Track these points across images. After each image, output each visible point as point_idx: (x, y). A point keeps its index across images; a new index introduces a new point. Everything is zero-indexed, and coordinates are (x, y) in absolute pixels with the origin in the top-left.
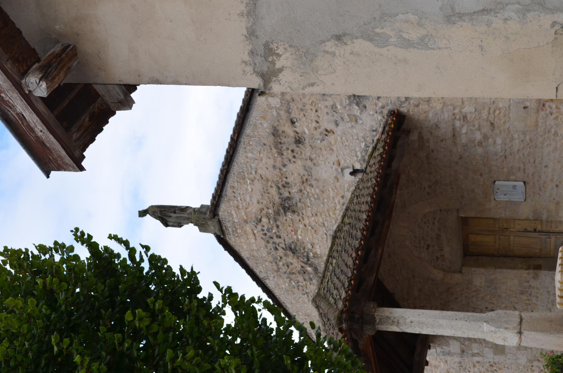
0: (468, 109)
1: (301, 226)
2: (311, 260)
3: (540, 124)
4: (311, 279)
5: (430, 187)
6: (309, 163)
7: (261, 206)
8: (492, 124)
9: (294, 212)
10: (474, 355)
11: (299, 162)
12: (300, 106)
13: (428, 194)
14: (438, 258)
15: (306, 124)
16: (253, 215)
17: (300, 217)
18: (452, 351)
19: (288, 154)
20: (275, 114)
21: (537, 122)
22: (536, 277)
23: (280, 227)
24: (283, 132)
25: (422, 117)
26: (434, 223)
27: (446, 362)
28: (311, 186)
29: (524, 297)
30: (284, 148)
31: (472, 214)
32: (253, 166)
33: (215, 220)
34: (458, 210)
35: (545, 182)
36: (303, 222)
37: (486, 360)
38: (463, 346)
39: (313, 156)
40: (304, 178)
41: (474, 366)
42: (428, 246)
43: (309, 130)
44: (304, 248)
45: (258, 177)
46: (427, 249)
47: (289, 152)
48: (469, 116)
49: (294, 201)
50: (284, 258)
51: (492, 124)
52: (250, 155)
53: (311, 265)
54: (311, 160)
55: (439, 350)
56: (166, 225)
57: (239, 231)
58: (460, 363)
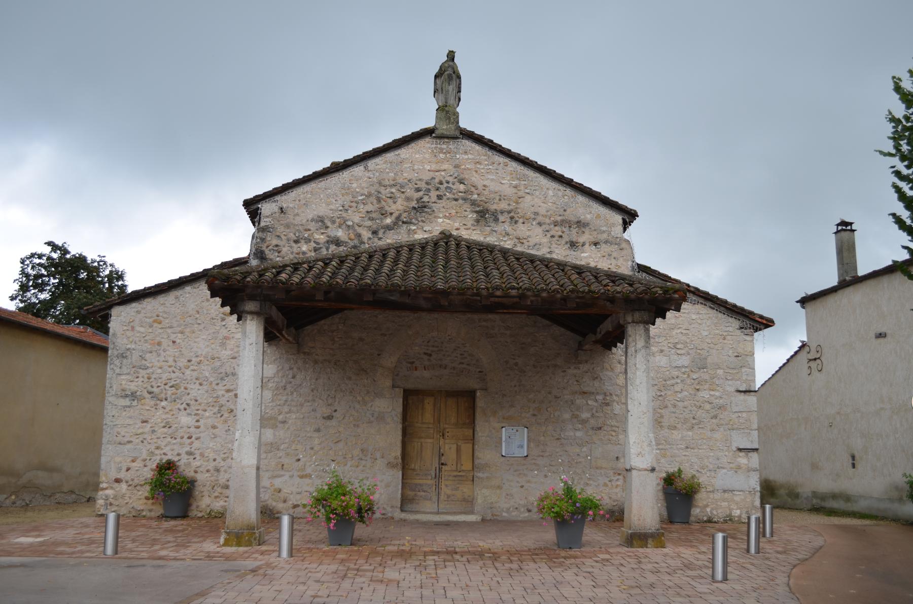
0: (617, 408)
1: (457, 225)
2: (405, 226)
3: (598, 471)
5: (516, 364)
7: (480, 187)
8: (600, 428)
9: (478, 221)
11: (545, 240)
12: (614, 254)
13: (507, 362)
14: (413, 363)
15: (593, 256)
16: (467, 177)
17: (469, 226)
19: (557, 231)
20: (604, 229)
21: (601, 468)
22: (391, 465)
23: (455, 202)
24: (584, 232)
25: (607, 365)
29: (356, 452)
30: (564, 229)
31: (480, 403)
32: (537, 193)
33: (457, 133)
35: (525, 475)
36: (462, 228)
40: (524, 241)
41: (228, 391)
42: (430, 355)
43: (585, 258)
44: (423, 221)
45: (520, 194)
46: (425, 354)
47: (560, 233)
48: (609, 408)
50: (403, 196)
51: (600, 428)
53: (395, 223)
56: (436, 77)
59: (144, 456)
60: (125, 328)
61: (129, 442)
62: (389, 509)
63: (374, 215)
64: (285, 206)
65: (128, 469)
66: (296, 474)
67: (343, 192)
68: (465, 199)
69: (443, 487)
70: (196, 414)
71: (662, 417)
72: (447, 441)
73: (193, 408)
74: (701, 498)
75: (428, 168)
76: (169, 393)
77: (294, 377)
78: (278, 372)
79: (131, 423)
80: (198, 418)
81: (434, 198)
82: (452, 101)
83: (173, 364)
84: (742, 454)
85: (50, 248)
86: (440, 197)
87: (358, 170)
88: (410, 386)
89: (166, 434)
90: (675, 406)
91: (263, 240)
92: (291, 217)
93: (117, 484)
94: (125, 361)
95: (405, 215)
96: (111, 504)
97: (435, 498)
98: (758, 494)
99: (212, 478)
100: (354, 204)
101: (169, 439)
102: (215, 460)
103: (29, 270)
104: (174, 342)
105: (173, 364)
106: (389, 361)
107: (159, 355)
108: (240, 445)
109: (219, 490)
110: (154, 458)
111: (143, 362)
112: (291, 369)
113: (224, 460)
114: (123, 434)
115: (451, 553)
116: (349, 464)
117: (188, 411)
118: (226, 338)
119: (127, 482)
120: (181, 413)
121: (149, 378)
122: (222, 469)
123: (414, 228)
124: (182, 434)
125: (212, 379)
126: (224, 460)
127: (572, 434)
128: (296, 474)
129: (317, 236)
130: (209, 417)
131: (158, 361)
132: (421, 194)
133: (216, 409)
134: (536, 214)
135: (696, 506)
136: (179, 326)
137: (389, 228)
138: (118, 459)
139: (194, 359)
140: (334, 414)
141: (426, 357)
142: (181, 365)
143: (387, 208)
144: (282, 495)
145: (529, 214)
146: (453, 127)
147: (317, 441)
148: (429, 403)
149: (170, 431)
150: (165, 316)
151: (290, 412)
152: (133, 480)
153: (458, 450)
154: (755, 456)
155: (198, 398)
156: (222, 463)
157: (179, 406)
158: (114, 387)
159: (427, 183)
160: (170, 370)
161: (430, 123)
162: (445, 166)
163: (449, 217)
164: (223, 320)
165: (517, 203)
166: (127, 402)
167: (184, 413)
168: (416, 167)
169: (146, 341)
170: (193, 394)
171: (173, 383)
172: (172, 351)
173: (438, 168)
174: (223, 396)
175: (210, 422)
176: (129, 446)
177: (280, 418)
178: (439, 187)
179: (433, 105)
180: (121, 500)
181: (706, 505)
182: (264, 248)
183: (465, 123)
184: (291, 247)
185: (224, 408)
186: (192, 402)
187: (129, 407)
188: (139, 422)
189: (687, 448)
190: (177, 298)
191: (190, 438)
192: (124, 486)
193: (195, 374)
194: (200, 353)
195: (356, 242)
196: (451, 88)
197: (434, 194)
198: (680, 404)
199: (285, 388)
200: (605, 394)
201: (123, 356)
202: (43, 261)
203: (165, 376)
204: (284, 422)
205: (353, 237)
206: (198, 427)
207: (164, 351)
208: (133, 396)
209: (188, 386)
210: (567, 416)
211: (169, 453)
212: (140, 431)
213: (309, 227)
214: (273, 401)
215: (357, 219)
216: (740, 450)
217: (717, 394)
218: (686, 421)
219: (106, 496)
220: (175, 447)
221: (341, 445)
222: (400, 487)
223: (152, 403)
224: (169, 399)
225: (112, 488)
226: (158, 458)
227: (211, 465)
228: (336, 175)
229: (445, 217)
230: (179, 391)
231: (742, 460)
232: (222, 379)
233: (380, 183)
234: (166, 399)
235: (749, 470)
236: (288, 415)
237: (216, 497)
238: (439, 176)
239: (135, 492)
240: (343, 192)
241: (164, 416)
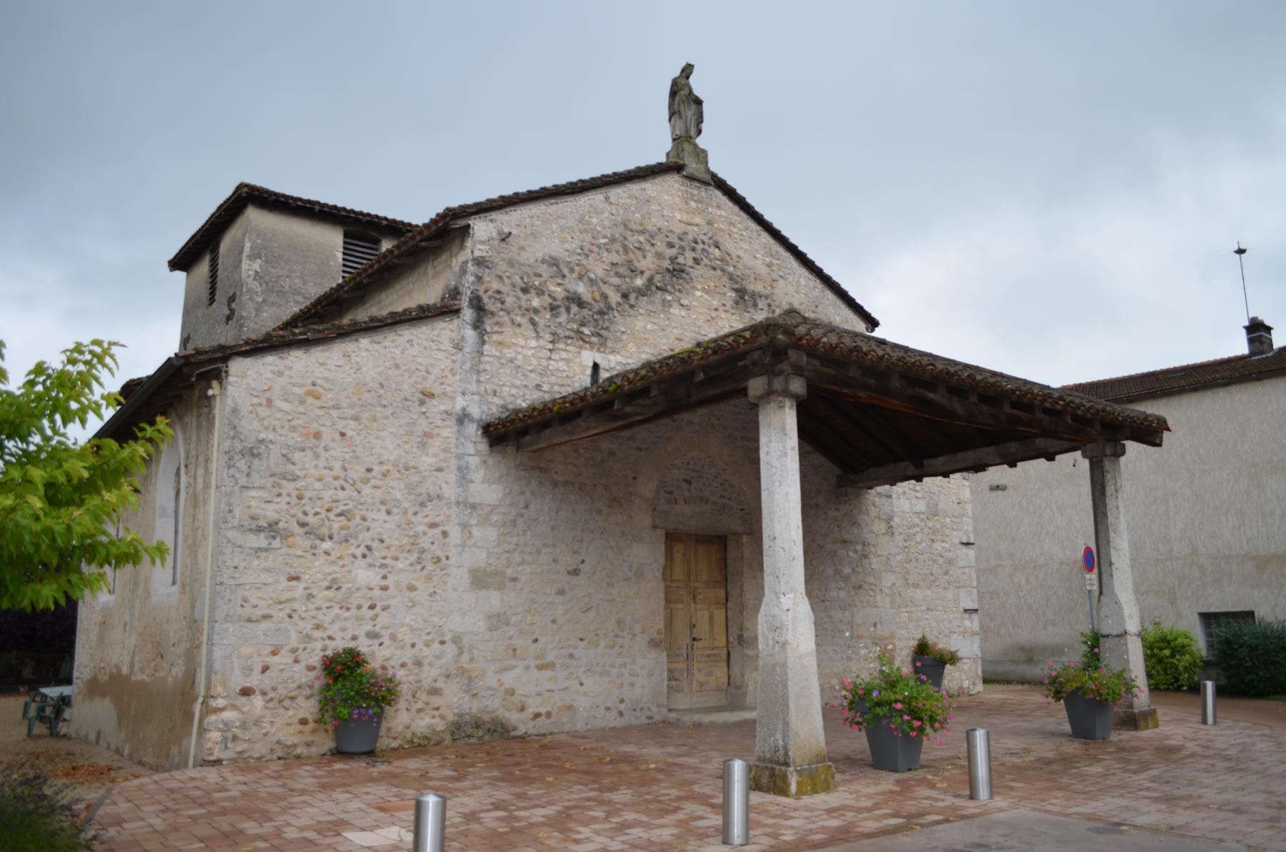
2: (660, 293)
7: (735, 259)
8: (860, 587)
9: (737, 303)
10: (464, 526)
14: (671, 493)
17: (728, 308)
18: (472, 486)
22: (654, 644)
26: (722, 497)
27: (440, 470)
33: (708, 178)
37: (453, 553)
38: (487, 510)
41: (433, 525)
44: (680, 291)
45: (774, 275)
46: (685, 480)
49: (751, 310)
58: (439, 497)
59: (294, 641)
60: (255, 400)
61: (266, 617)
62: (655, 709)
63: (621, 270)
65: (265, 669)
66: (533, 663)
67: (581, 227)
68: (723, 270)
69: (695, 672)
70: (382, 566)
72: (699, 606)
73: (377, 554)
75: (679, 217)
76: (336, 526)
77: (526, 507)
78: (505, 495)
79: (270, 580)
80: (384, 571)
81: (691, 262)
82: (693, 132)
83: (342, 474)
87: (596, 198)
89: (331, 600)
92: (515, 250)
93: (244, 699)
94: (256, 462)
95: (658, 277)
96: (235, 738)
99: (411, 678)
100: (594, 248)
101: (336, 611)
102: (413, 646)
104: (343, 434)
105: (342, 474)
106: (647, 488)
107: (317, 456)
108: (794, 619)
109: (423, 697)
110: (309, 646)
111: (290, 467)
112: (523, 493)
113: (427, 645)
114: (253, 601)
116: (602, 644)
117: (369, 560)
118: (427, 435)
119: (264, 693)
120: (357, 562)
121: (300, 498)
122: (426, 661)
123: (669, 298)
124: (359, 601)
125: (406, 505)
127: (835, 594)
128: (533, 663)
129: (553, 288)
130: (401, 571)
131: (316, 467)
136: (351, 406)
138: (245, 651)
139: (376, 468)
140: (582, 567)
141: (685, 486)
142: (355, 476)
143: (636, 263)
144: (515, 699)
147: (561, 610)
149: (339, 595)
150: (327, 385)
152: (274, 689)
153: (711, 618)
154: (975, 617)
155: (385, 537)
156: (426, 651)
157: (352, 550)
158: (237, 512)
159: (680, 239)
160: (337, 484)
162: (697, 220)
164: (422, 403)
165: (772, 287)
166: (261, 541)
167: (361, 562)
168: (665, 213)
169: (294, 429)
170: (377, 528)
171: (341, 508)
172: (339, 450)
173: (689, 220)
174: (425, 533)
175: (405, 579)
176: (265, 625)
177: (509, 572)
180: (254, 729)
182: (481, 293)
184: (518, 298)
185: (427, 556)
186: (375, 544)
187: (266, 550)
188: (283, 578)
190: (346, 355)
191: (372, 607)
192: (258, 701)
193: (379, 494)
194: (385, 458)
195: (602, 305)
197: (689, 255)
198: (921, 557)
199: (514, 523)
203: (328, 495)
205: (598, 297)
206: (385, 588)
207: (326, 449)
208: (272, 529)
209: (368, 514)
210: (830, 571)
211: (338, 636)
212: (287, 595)
213: (539, 271)
214: (498, 545)
216: (966, 611)
217: (947, 546)
219: (226, 724)
220: (349, 624)
221: (592, 615)
223: (308, 543)
224: (336, 538)
225: (234, 707)
226: (319, 645)
228: (570, 199)
229: (703, 290)
230: (352, 524)
232: (422, 505)
233: (626, 226)
234: (331, 538)
236: (519, 569)
237: (419, 711)
238: (693, 232)
239: (281, 711)
240: (581, 227)
241: (328, 569)
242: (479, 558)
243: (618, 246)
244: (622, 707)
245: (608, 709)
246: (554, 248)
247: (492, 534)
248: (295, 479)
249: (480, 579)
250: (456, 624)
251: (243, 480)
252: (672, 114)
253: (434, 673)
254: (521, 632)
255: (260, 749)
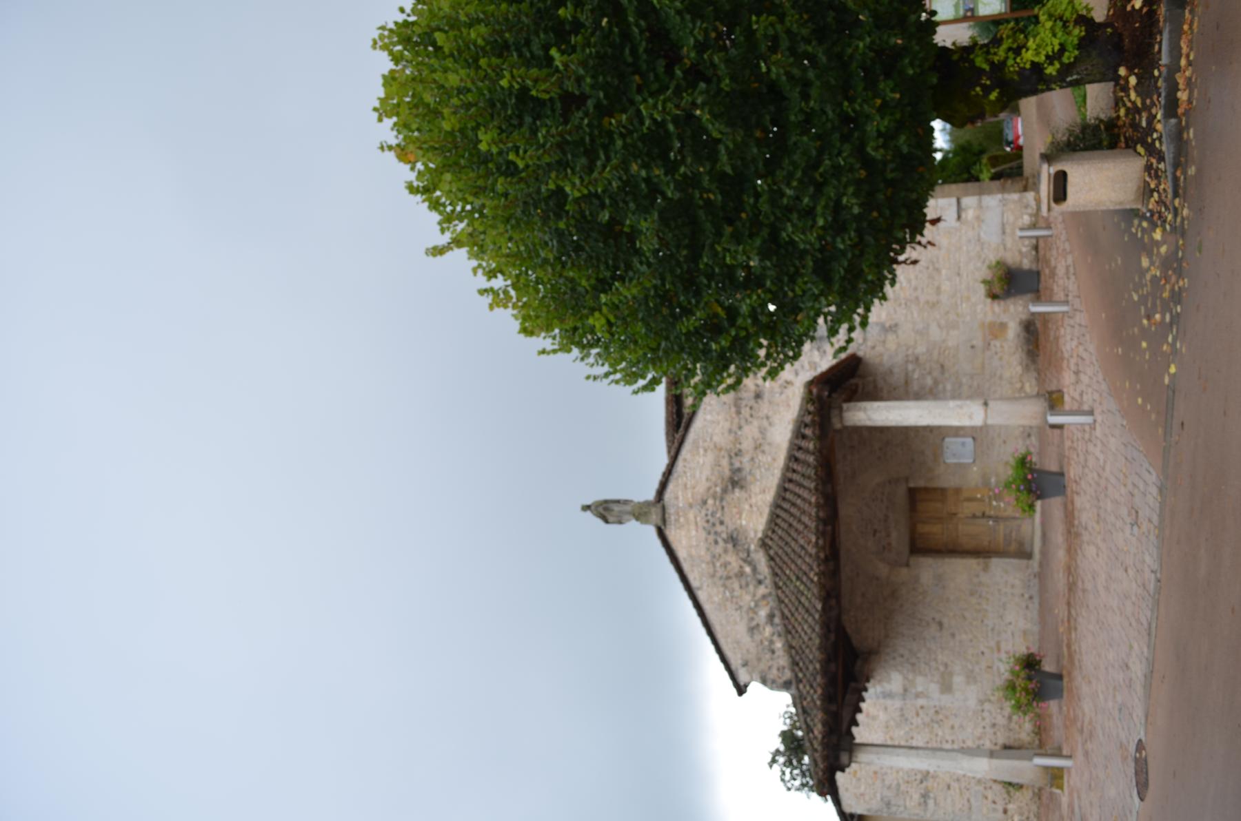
1: (747, 507)
2: (752, 555)
4: (747, 585)
5: (880, 449)
6: (765, 423)
7: (708, 484)
8: (942, 366)
9: (742, 487)
10: (917, 696)
14: (884, 548)
16: (699, 497)
19: (746, 412)
22: (986, 569)
25: (877, 361)
27: (886, 709)
28: (763, 452)
29: (974, 600)
33: (659, 505)
34: (907, 480)
39: (770, 414)
41: (918, 714)
45: (712, 446)
49: (744, 473)
52: (709, 417)
53: (750, 563)
54: (768, 418)
55: (879, 689)
56: (607, 522)
57: (682, 520)
58: (902, 709)
59: (981, 788)
63: (743, 583)
64: (740, 662)
65: (994, 802)
68: (722, 499)
71: (927, 302)
74: (1012, 258)
77: (902, 656)
82: (628, 508)
84: (963, 215)
85: (775, 766)
86: (722, 523)
87: (702, 596)
88: (906, 550)
90: (916, 289)
91: (773, 682)
93: (1009, 813)
94: (893, 802)
97: (1019, 522)
98: (1006, 196)
103: (797, 783)
106: (883, 570)
115: (1072, 587)
126: (983, 719)
132: (720, 540)
133: (936, 726)
134: (730, 431)
135: (1021, 262)
137: (754, 570)
138: (985, 811)
141: (878, 535)
145: (731, 438)
146: (653, 510)
147: (964, 636)
148: (923, 529)
151: (935, 660)
156: (987, 721)
161: (651, 531)
162: (691, 516)
163: (740, 513)
165: (721, 449)
166: (931, 802)
176: (972, 800)
177: (942, 668)
178: (712, 525)
179: (633, 525)
181: (1018, 255)
183: (651, 495)
189: (959, 274)
192: (1010, 807)
196: (616, 508)
197: (719, 528)
198: (914, 283)
199: (913, 665)
200: (907, 362)
201: (888, 804)
202: (788, 771)
204: (946, 665)
208: (925, 796)
214: (926, 675)
215: (748, 598)
216: (959, 217)
218: (931, 277)
221: (967, 614)
222: (1007, 560)
227: (989, 730)
231: (969, 214)
235: (980, 206)
238: (701, 523)
242: (934, 688)
243: (728, 583)
244: (1026, 596)
245: (1027, 607)
246: (741, 629)
247: (920, 680)
248: (898, 785)
249: (947, 688)
250: (972, 703)
251: (902, 809)
252: (620, 522)
253: (999, 717)
254: (977, 663)
255: (1034, 808)
